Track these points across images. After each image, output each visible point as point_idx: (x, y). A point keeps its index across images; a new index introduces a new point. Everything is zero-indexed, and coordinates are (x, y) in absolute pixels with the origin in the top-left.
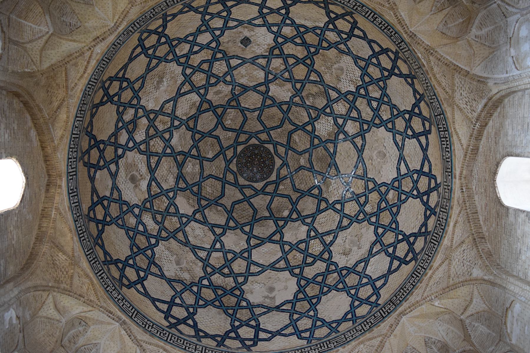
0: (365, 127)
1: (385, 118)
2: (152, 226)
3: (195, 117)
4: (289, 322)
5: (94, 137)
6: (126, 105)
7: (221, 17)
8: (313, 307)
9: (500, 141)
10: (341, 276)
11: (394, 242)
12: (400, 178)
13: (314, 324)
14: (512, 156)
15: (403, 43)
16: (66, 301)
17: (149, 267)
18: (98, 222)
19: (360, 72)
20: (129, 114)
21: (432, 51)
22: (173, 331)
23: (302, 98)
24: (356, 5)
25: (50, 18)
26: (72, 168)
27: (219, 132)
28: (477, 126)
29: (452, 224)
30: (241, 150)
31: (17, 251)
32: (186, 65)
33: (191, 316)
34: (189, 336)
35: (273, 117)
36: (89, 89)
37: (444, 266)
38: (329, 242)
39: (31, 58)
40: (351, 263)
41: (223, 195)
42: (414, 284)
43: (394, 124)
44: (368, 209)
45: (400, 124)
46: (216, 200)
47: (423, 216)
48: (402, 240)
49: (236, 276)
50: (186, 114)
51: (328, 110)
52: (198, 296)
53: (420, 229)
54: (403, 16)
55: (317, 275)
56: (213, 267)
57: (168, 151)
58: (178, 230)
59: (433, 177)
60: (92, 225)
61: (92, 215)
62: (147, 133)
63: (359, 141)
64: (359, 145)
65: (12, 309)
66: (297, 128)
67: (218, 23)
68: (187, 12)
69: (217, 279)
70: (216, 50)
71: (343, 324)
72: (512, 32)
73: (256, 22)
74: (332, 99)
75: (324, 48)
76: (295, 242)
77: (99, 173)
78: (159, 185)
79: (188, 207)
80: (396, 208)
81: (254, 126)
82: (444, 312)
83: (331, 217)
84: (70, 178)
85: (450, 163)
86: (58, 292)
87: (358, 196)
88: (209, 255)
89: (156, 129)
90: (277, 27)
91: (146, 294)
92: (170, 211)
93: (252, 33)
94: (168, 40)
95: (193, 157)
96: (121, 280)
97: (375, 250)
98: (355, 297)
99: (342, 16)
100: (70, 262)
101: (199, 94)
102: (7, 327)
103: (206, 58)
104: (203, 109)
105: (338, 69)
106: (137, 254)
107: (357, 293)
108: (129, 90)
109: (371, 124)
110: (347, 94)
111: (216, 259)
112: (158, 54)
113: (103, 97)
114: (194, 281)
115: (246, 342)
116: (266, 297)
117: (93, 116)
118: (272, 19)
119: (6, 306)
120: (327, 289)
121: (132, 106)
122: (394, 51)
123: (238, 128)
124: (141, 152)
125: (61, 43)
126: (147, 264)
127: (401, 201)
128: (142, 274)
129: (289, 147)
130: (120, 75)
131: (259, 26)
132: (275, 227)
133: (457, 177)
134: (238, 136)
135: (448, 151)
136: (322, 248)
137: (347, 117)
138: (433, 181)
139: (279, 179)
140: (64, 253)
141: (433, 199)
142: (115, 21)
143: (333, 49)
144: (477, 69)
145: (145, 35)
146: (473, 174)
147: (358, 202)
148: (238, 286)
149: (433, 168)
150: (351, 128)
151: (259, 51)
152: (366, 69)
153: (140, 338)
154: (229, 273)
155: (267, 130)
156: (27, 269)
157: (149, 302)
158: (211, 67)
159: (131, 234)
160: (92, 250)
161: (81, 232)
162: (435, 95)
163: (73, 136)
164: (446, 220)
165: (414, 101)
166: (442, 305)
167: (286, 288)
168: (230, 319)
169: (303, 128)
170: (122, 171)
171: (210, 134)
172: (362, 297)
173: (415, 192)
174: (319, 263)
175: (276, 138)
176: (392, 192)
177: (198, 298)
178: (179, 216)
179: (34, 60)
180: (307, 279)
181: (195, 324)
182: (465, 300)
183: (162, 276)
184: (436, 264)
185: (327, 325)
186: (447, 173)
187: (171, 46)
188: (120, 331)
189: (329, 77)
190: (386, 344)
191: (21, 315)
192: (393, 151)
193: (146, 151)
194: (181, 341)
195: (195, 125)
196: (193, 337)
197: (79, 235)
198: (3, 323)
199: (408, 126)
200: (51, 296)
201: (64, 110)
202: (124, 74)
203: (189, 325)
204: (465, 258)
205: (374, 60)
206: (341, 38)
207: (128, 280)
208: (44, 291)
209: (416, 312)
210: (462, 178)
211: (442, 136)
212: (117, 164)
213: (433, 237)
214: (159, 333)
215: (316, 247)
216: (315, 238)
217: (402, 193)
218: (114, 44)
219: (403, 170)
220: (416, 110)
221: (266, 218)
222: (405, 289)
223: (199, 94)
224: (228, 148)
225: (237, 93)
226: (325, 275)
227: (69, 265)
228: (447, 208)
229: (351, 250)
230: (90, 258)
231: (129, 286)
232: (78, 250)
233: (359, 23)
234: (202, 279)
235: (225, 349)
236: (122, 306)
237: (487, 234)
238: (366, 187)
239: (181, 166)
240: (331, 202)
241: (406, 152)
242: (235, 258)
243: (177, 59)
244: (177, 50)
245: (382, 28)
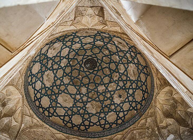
0: (75, 101)
1: (74, 109)
29: (38, 120)
37: (29, 113)
44: (55, 88)
50: (120, 66)
51: (87, 95)
66: (89, 83)
73: (122, 104)
81: (100, 73)
93: (120, 100)
97: (43, 85)
129: (87, 76)
134: (101, 67)
155: (96, 75)
169: (88, 84)
171: (109, 63)
176: (55, 98)
209: (21, 101)
221: (74, 57)
239: (110, 51)
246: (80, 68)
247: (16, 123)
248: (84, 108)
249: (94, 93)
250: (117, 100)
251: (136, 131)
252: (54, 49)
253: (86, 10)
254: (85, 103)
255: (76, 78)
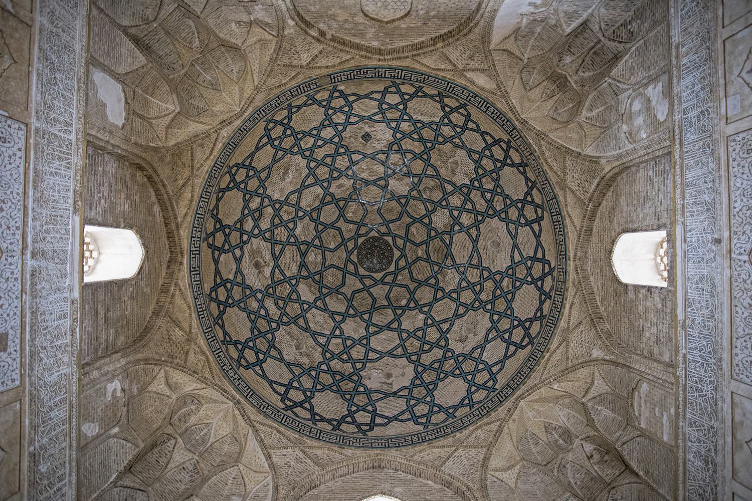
1: (498, 208)
2: (273, 311)
3: (319, 209)
4: (406, 407)
5: (220, 221)
6: (253, 194)
7: (343, 112)
8: (430, 393)
9: (615, 219)
10: (458, 363)
11: (510, 328)
12: (514, 266)
13: (431, 410)
14: (628, 232)
15: (515, 131)
16: (179, 377)
17: (268, 350)
18: (219, 303)
19: (474, 165)
20: (255, 204)
21: (543, 136)
22: (289, 413)
23: (419, 192)
24: (469, 95)
25: (178, 97)
26: (195, 247)
27: (341, 224)
28: (590, 206)
29: (568, 306)
30: (361, 241)
31: (131, 322)
32: (310, 159)
33: (308, 399)
34: (305, 419)
35: (391, 211)
36: (215, 172)
37: (561, 348)
38: (445, 329)
39: (156, 133)
40: (467, 350)
41: (343, 284)
42: (531, 367)
43: (507, 213)
44: (483, 296)
45: (513, 213)
46: (337, 289)
47: (538, 301)
48: (518, 326)
49: (354, 362)
50: (310, 206)
52: (316, 381)
53: (536, 314)
54: (515, 103)
55: (434, 362)
56: (332, 353)
57: (292, 240)
58: (300, 316)
59: (547, 262)
60: (214, 305)
61: (214, 295)
62: (272, 222)
63: (474, 232)
64: (474, 236)
65: (116, 381)
66: (415, 221)
67: (340, 118)
68: (311, 105)
69: (335, 364)
70: (339, 145)
71: (460, 409)
72: (624, 109)
73: (376, 118)
74: (448, 192)
75: (440, 143)
76: (412, 330)
77: (223, 256)
78: (282, 272)
79: (309, 294)
80: (511, 295)
82: (563, 396)
83: (448, 306)
84: (192, 256)
85: (563, 246)
86: (171, 367)
87: (473, 285)
88: (328, 341)
89: (280, 218)
90: (396, 123)
91: (264, 376)
92: (292, 297)
93: (373, 129)
94: (293, 132)
95: (315, 246)
96: (239, 361)
98: (471, 383)
99: (456, 109)
100: (187, 337)
101: (322, 187)
102: (109, 399)
103: (330, 153)
104: (325, 201)
105: (453, 163)
106: (257, 337)
107: (473, 379)
108: (256, 178)
109: (485, 215)
110: (462, 186)
111: (335, 345)
112: (283, 145)
113: (230, 183)
114: (312, 365)
115: (362, 426)
116: (384, 383)
117: (218, 200)
118: (390, 115)
119: (109, 376)
120: (444, 375)
121: (258, 195)
122: (506, 140)
123: (359, 221)
124: (265, 239)
125: (188, 123)
126: (267, 347)
127: (515, 288)
128: (261, 356)
129: (407, 238)
130: (247, 163)
131: (379, 122)
132: (393, 315)
133: (572, 259)
134: (358, 229)
135: (562, 235)
136: (439, 336)
137: (462, 209)
138: (547, 266)
139: (398, 270)
140: (181, 329)
141: (548, 283)
142: (241, 106)
143: (448, 143)
144: (588, 149)
145: (271, 125)
146: (587, 256)
147: (474, 291)
148: (356, 372)
149: (546, 253)
150: (466, 219)
151: (379, 147)
152: (479, 162)
153: (253, 419)
154: (347, 358)
156: (140, 340)
157: (266, 384)
158: (334, 161)
159: (253, 317)
160: (211, 329)
161: (201, 310)
162: (547, 180)
163: (198, 215)
164: (561, 302)
165: (526, 189)
166: (562, 388)
167: (403, 374)
168: (347, 404)
169: (420, 220)
170: (247, 257)
171: (332, 226)
172: (478, 383)
173: (529, 279)
174: (436, 350)
175: (394, 230)
176: (506, 279)
177: (316, 382)
178: (301, 302)
179: (160, 136)
180: (424, 367)
181: (312, 408)
182: (586, 382)
183: (282, 360)
184: (553, 347)
185: (444, 410)
186: (561, 256)
187: (296, 139)
188: (234, 411)
189: (444, 171)
190: (505, 428)
191: (127, 387)
192: (507, 240)
193: (271, 239)
194: (296, 423)
195: (319, 217)
196: (309, 420)
197: (198, 312)
198: (105, 395)
199: (521, 215)
200: (162, 371)
201: (188, 189)
202: (250, 163)
203: (306, 409)
204: (583, 339)
205: (487, 153)
206: (456, 132)
207: (247, 362)
208: (155, 364)
209: (535, 396)
210: (577, 259)
211: (554, 221)
212: (242, 249)
213: (549, 321)
214: (274, 414)
215: (433, 335)
216: (432, 325)
217: (516, 280)
218: (240, 129)
219: (517, 258)
220: (529, 199)
221: (384, 307)
222: (522, 373)
223: (323, 187)
224: (350, 239)
225: (357, 186)
226: (442, 361)
227: (185, 341)
228: (562, 290)
229: (467, 337)
230: (208, 336)
231: (248, 367)
232: (196, 327)
233: (472, 115)
234: (320, 364)
235: (341, 433)
236: (238, 385)
237: (605, 314)
238: (481, 276)
239: (304, 255)
240: (447, 291)
241: (520, 240)
242: (354, 344)
243: (302, 152)
244: (302, 143)
245: (495, 118)
246: (404, 268)
247: (596, 382)
248: (478, 185)
249: (425, 193)
250: (383, 134)
251: (370, 45)
252: (389, 376)
253: (181, 467)
254: (465, 190)
255: (428, 260)
